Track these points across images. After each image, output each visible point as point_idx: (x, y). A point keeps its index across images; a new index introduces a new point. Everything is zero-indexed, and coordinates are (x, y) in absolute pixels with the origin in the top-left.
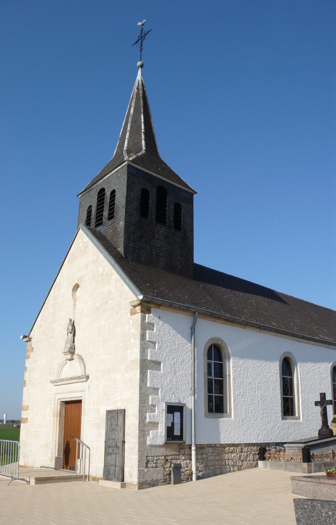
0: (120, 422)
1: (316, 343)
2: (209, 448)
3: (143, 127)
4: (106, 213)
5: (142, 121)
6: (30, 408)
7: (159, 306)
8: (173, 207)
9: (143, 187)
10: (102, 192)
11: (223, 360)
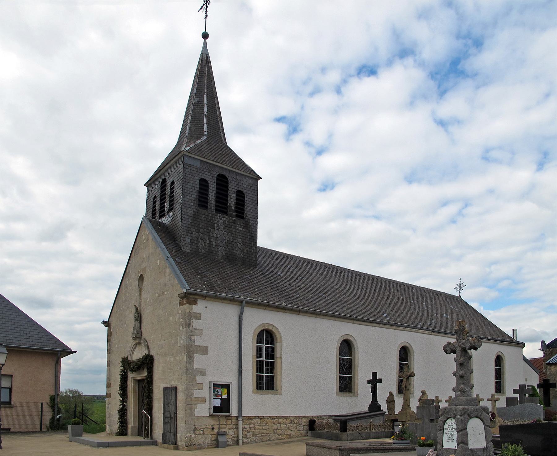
0: (173, 397)
1: (381, 326)
2: (257, 420)
3: (206, 110)
4: (167, 204)
5: (205, 102)
6: (112, 385)
7: (205, 297)
8: (235, 195)
9: (201, 177)
10: (164, 181)
11: (275, 344)
